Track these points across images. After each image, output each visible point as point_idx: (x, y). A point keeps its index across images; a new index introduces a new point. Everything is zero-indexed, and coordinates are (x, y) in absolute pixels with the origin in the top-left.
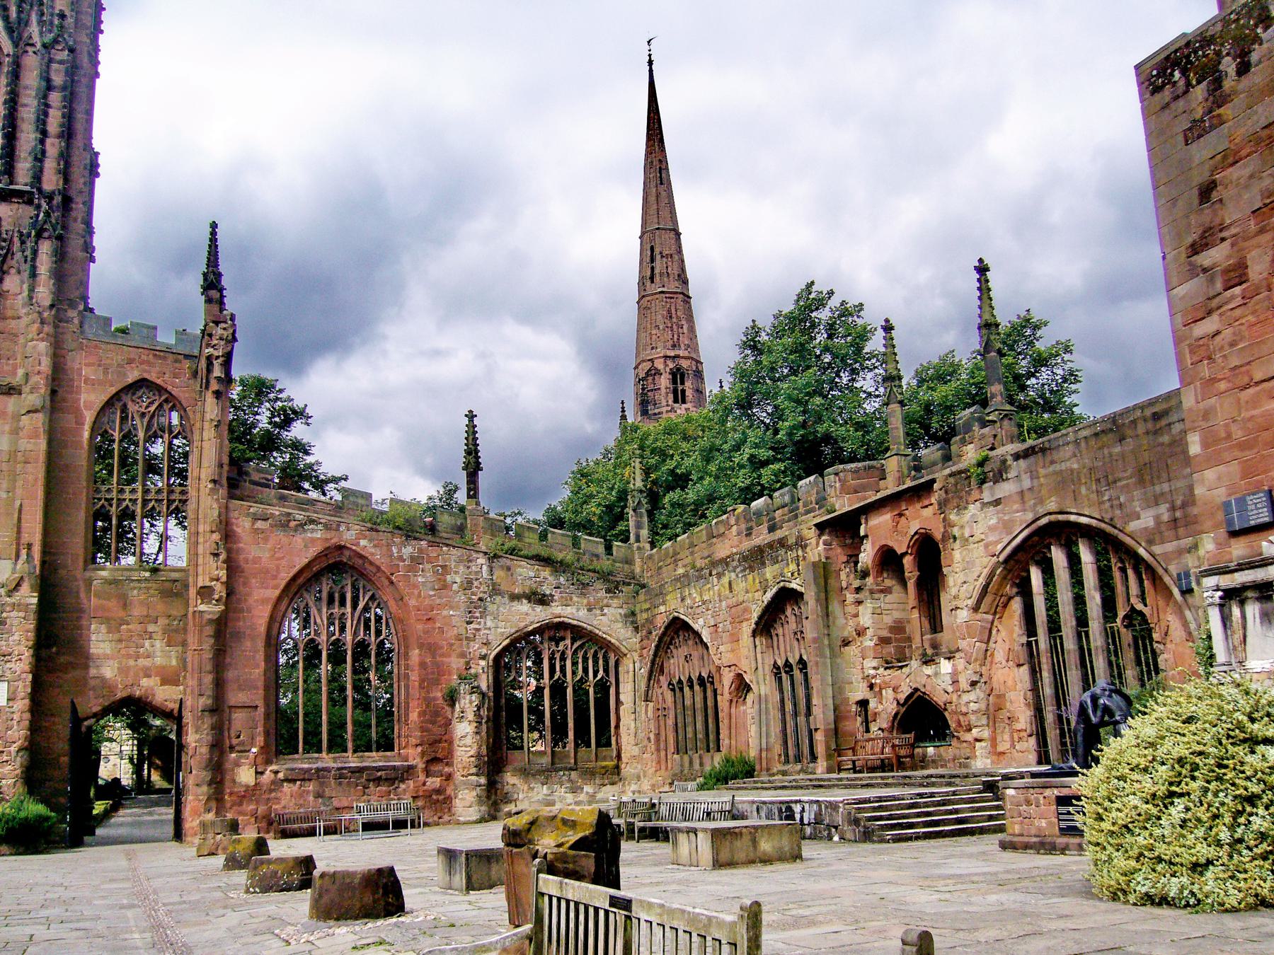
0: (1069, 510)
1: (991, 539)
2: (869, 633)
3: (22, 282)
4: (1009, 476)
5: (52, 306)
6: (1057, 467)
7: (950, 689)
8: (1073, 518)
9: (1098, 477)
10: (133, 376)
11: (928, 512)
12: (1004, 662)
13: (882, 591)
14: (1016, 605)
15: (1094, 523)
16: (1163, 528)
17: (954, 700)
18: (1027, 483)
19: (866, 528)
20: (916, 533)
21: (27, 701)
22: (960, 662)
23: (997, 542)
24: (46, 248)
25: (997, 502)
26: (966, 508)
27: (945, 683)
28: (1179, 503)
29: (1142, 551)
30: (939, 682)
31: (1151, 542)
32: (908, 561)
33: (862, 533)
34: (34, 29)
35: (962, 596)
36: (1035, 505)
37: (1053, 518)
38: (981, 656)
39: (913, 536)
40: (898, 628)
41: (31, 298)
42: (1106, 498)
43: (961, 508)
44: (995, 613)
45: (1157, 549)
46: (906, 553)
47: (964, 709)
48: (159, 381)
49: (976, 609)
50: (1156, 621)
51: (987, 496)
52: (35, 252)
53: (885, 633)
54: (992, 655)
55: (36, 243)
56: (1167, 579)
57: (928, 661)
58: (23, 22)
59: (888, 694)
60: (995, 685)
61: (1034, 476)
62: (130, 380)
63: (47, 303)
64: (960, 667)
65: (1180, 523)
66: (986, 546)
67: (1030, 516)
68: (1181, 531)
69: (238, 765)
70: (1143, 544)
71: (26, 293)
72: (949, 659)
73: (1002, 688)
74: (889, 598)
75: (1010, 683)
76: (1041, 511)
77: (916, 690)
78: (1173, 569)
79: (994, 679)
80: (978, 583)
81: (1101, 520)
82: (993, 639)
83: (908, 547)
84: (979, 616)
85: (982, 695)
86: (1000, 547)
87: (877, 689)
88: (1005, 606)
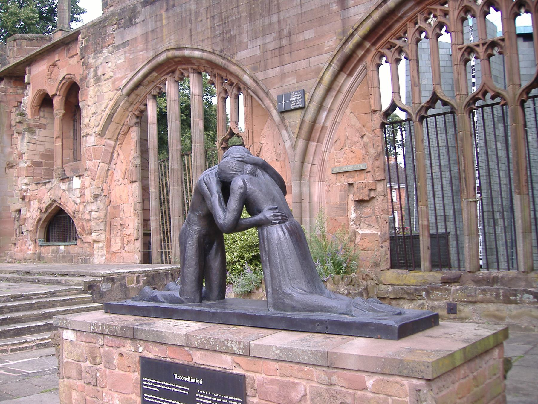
0: (184, 46)
1: (118, 75)
2: (25, 157)
4: (138, 21)
6: (178, 9)
7: (78, 201)
8: (187, 53)
9: (212, 14)
11: (74, 60)
12: (121, 180)
13: (38, 126)
14: (134, 134)
15: (205, 55)
16: (269, 55)
17: (81, 209)
18: (151, 25)
19: (29, 77)
20: (64, 78)
22: (87, 180)
23: (122, 79)
25: (125, 44)
26: (101, 52)
27: (75, 196)
28: (285, 32)
29: (246, 78)
30: (71, 195)
31: (255, 69)
32: (56, 101)
33: (26, 80)
35: (92, 124)
36: (156, 44)
37: (170, 54)
38: (103, 174)
39: (61, 81)
40: (49, 156)
42: (218, 32)
43: (97, 51)
44: (117, 139)
45: (260, 76)
46: (56, 95)
47: (87, 217)
49: (101, 134)
50: (250, 143)
51: (118, 41)
53: (37, 159)
54: (112, 174)
56: (267, 102)
57: (64, 179)
59: (35, 205)
60: (113, 198)
61: (158, 18)
64: (87, 184)
65: (286, 50)
66: (114, 83)
67: (151, 54)
68: (286, 57)
70: (248, 71)
72: (79, 176)
73: (118, 201)
74: (43, 132)
75: (124, 197)
76: (161, 49)
77: (55, 201)
78: (274, 93)
79: (112, 194)
80: (105, 114)
81: (213, 53)
82: (114, 161)
83: (57, 90)
84: (104, 141)
85: (102, 206)
86: (124, 82)
87: (27, 200)
88: (125, 134)
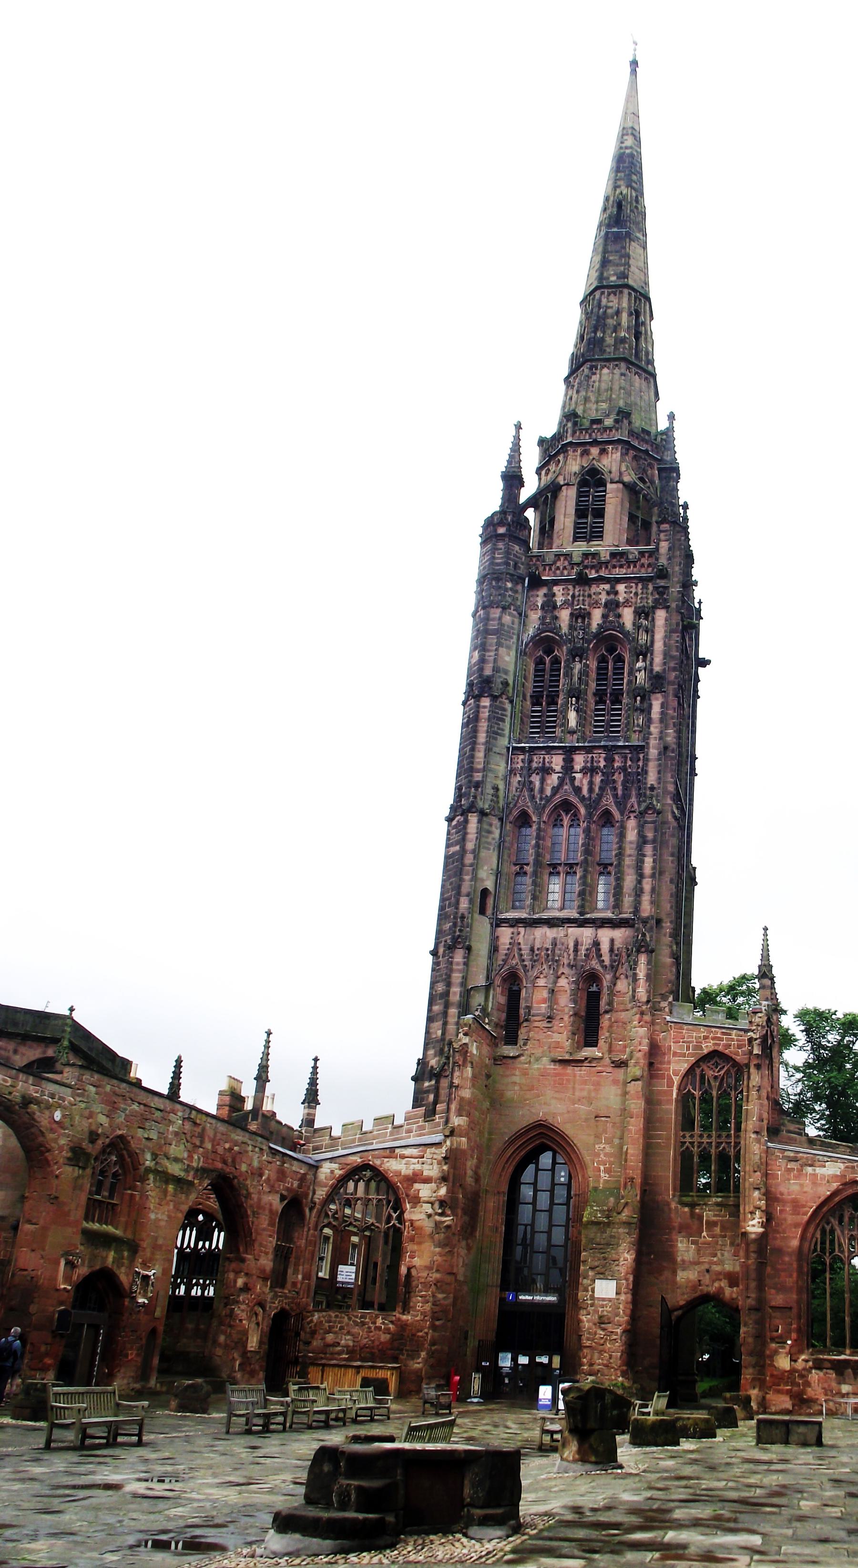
3: (629, 984)
5: (648, 1002)
10: (707, 1047)
21: (629, 1296)
24: (643, 959)
34: (633, 800)
41: (634, 997)
48: (727, 1052)
52: (636, 963)
55: (637, 957)
58: (626, 797)
62: (705, 1051)
63: (644, 999)
69: (776, 1352)
71: (631, 993)
